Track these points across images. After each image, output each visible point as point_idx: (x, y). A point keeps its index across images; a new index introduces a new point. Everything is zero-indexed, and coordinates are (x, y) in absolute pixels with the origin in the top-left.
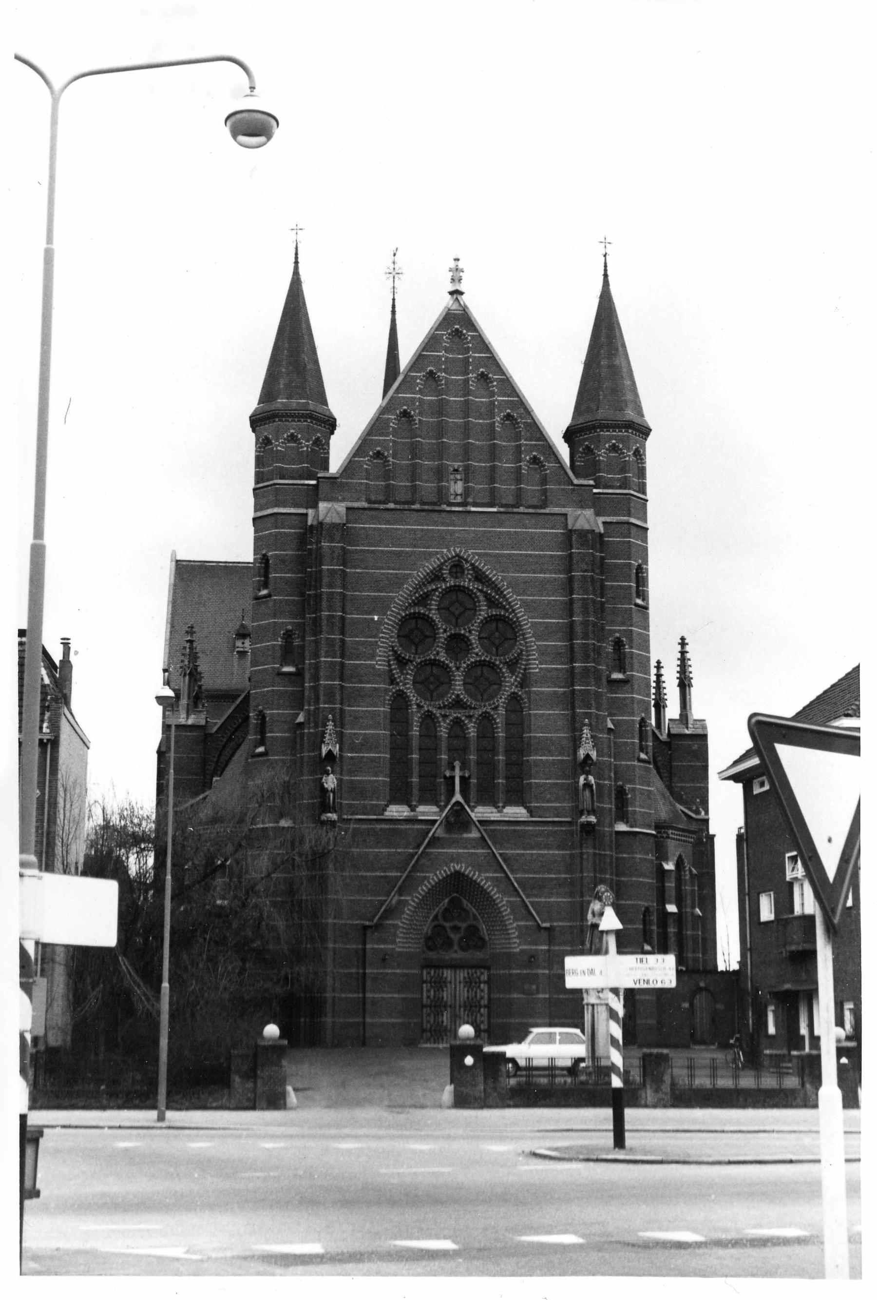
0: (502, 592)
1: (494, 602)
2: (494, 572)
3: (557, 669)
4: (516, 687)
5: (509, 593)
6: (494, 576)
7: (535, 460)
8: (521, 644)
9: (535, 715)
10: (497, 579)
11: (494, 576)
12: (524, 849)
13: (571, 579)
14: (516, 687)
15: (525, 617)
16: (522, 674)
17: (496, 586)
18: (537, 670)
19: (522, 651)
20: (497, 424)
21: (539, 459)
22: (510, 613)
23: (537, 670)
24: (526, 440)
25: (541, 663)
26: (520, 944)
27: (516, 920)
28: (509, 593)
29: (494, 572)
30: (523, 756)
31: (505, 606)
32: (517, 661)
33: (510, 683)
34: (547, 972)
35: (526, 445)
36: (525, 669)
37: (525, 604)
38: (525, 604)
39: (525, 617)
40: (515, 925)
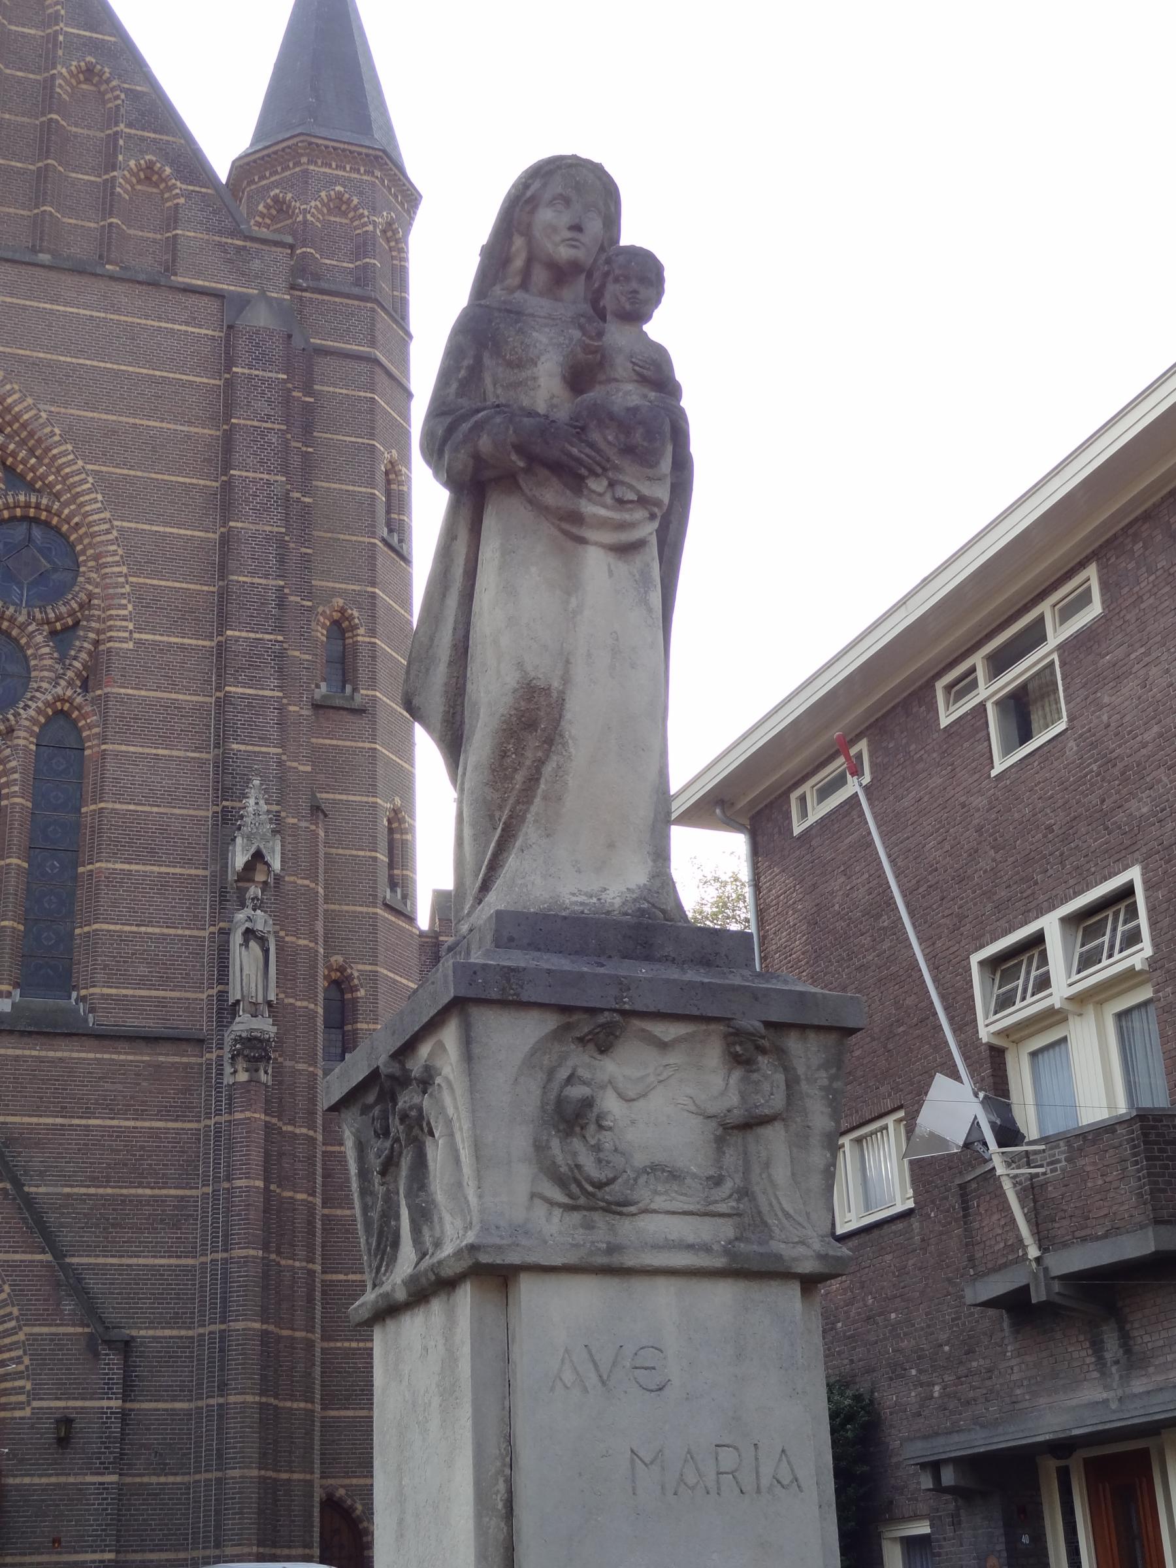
0: (48, 450)
1: (22, 477)
2: (30, 401)
3: (182, 648)
4: (70, 683)
5: (64, 454)
6: (28, 409)
7: (149, 174)
8: (89, 581)
9: (117, 754)
10: (37, 417)
11: (28, 409)
12: (63, 1112)
13: (228, 442)
14: (70, 683)
15: (107, 515)
16: (90, 653)
17: (31, 434)
18: (130, 645)
19: (91, 596)
20: (59, 81)
21: (159, 173)
22: (66, 504)
23: (130, 645)
24: (127, 126)
25: (140, 630)
26: (34, 1395)
27: (25, 1320)
28: (64, 454)
29: (30, 401)
30: (76, 864)
31: (50, 486)
32: (77, 624)
33: (48, 684)
34: (114, 1478)
35: (129, 136)
36: (97, 643)
37: (104, 483)
38: (104, 483)
39: (107, 515)
40: (21, 1336)
